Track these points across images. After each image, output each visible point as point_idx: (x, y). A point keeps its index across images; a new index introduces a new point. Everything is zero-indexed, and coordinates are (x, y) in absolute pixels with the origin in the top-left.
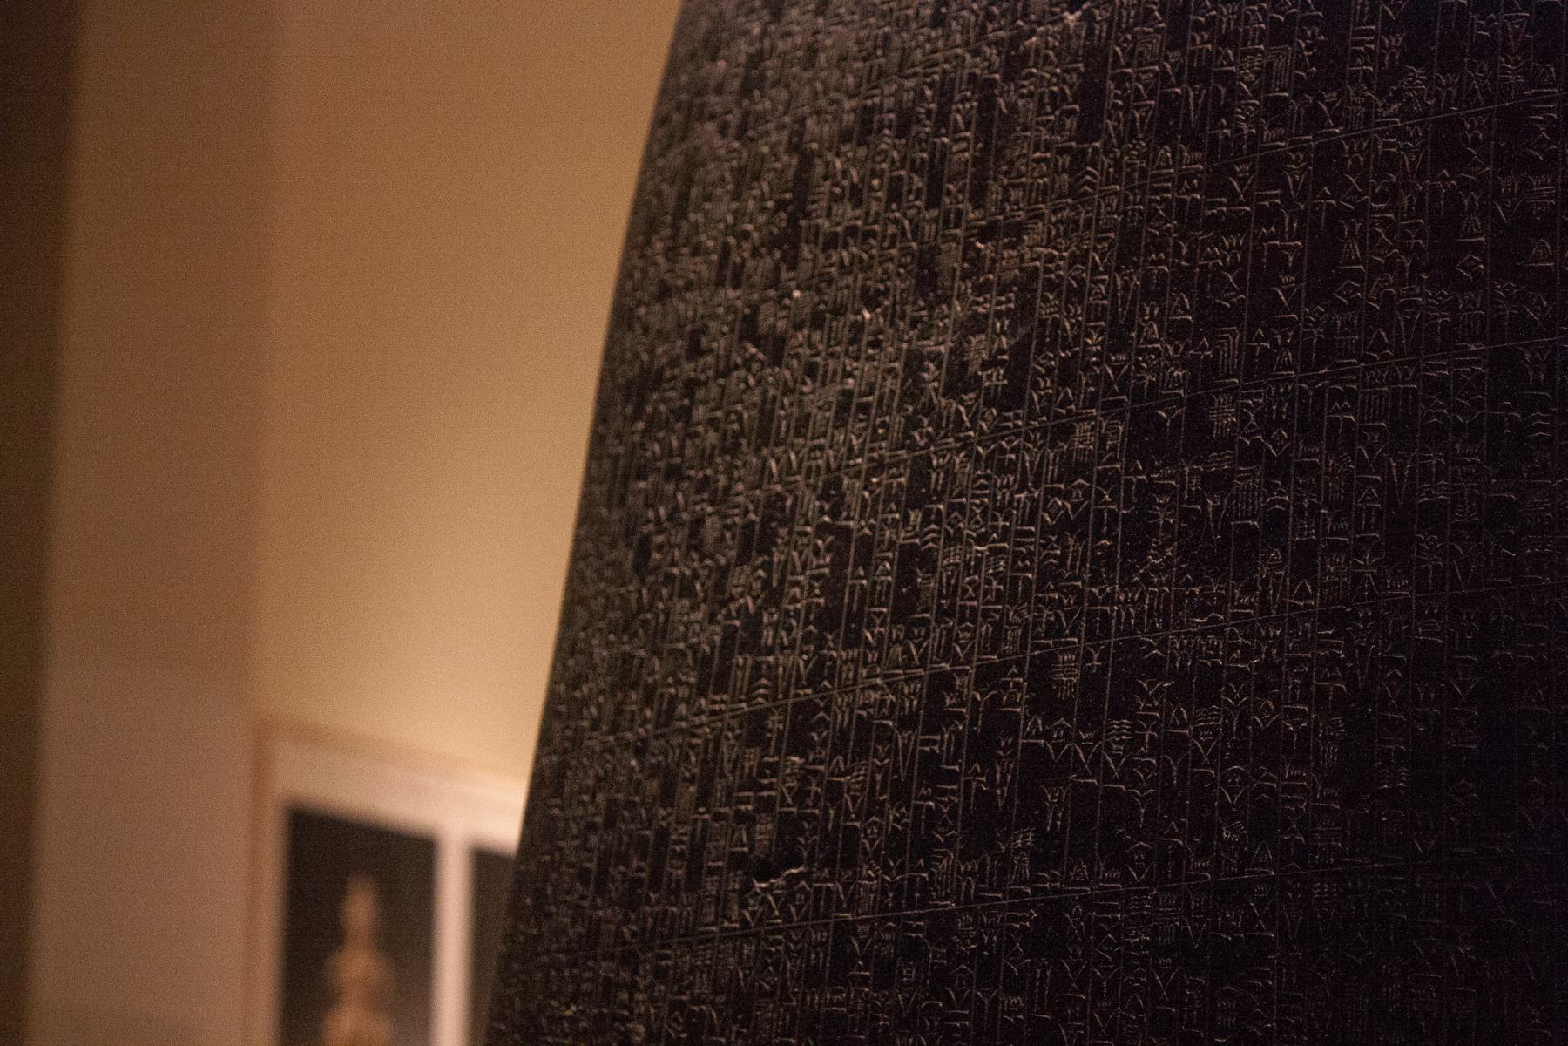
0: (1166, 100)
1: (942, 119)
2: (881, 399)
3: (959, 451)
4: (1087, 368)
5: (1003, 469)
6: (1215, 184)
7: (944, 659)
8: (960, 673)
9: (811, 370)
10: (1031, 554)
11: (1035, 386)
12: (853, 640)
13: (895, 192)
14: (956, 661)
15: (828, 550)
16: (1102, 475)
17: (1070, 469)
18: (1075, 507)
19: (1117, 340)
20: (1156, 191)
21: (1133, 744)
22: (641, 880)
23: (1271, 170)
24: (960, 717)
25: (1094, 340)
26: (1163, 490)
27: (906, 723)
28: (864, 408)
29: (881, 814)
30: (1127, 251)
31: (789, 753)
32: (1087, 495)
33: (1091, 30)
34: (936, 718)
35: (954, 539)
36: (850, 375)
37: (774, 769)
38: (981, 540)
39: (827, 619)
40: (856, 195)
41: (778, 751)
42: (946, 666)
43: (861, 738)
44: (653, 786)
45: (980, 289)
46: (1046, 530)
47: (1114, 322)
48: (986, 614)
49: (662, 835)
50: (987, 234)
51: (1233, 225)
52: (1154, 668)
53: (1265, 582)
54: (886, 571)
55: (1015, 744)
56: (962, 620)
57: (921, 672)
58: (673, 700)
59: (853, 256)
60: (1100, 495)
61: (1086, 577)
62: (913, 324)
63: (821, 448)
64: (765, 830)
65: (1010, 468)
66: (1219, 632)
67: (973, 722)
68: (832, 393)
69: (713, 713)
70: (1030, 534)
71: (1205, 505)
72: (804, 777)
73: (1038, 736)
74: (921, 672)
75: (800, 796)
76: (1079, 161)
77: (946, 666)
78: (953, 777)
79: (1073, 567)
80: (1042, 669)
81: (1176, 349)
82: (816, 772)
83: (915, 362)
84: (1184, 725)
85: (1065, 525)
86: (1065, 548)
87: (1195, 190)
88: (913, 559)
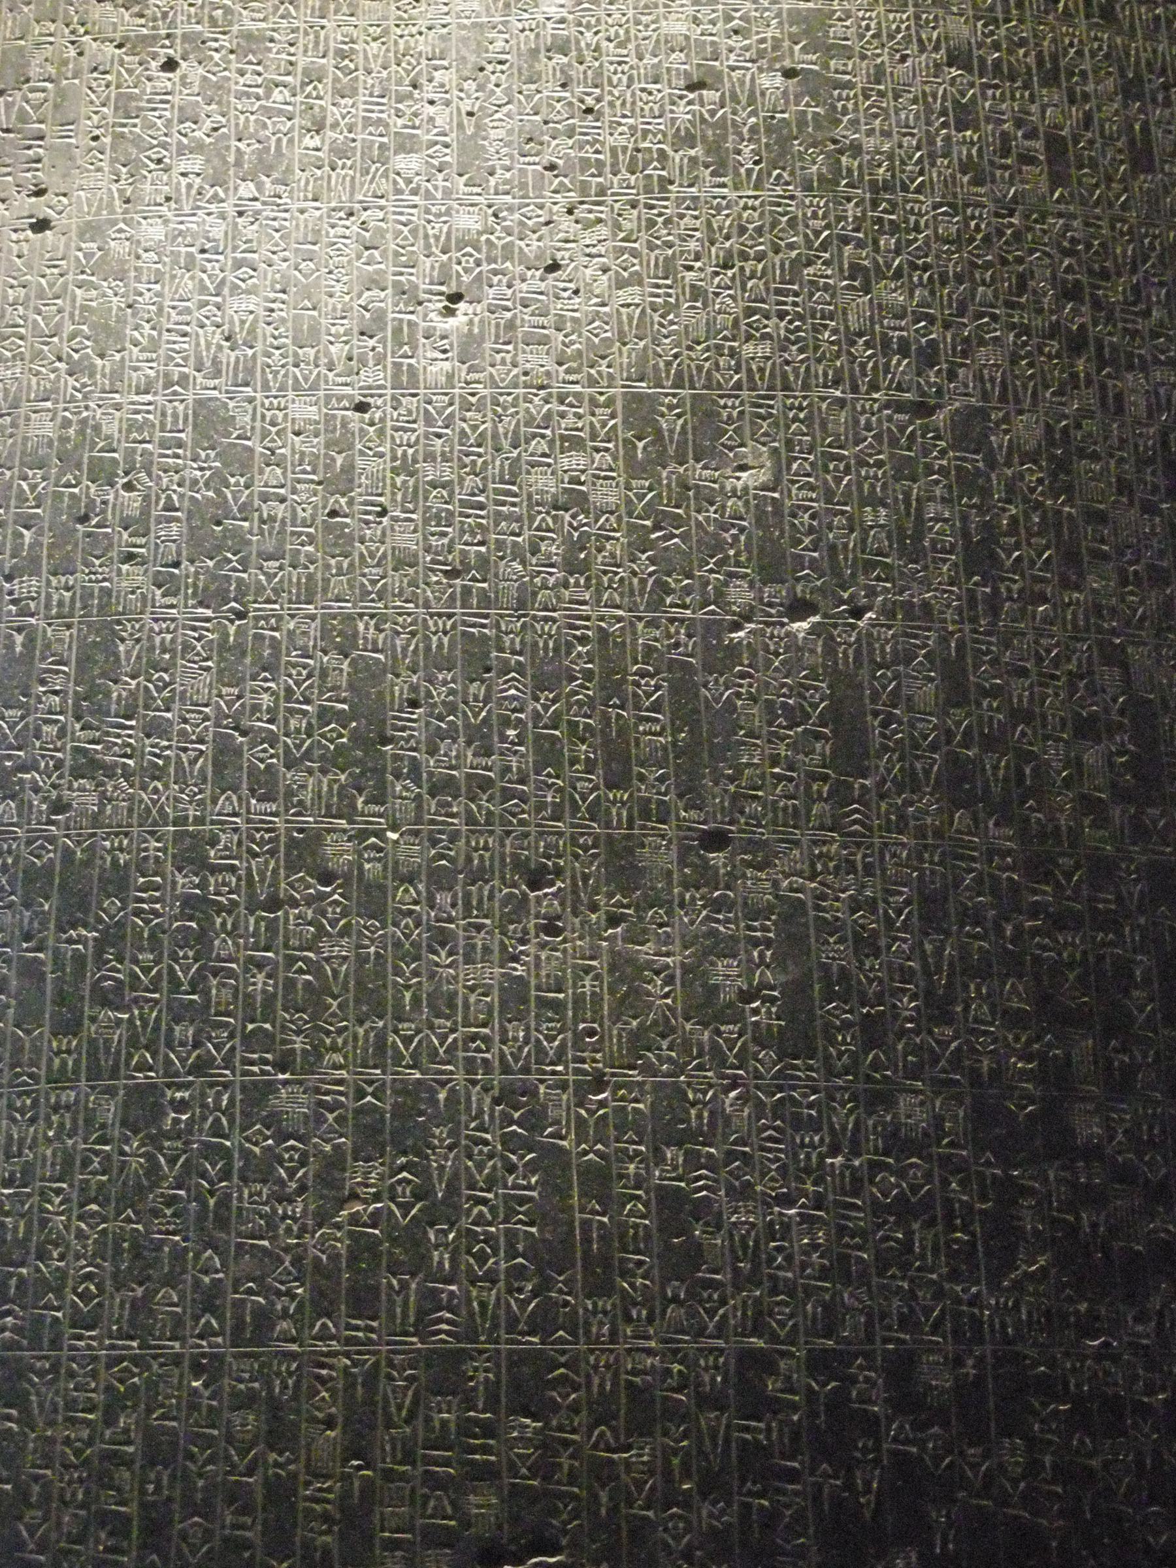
0: (953, 760)
1: (612, 685)
2: (579, 1000)
3: (727, 1090)
4: (903, 1032)
5: (798, 1123)
6: (1039, 868)
7: (756, 1331)
8: (783, 1354)
9: (442, 938)
10: (863, 1233)
11: (832, 1041)
12: (600, 1287)
13: (548, 754)
14: (774, 1338)
15: (532, 1168)
16: (945, 1161)
17: (898, 1143)
18: (914, 1189)
19: (938, 1008)
20: (962, 858)
21: (1033, 1467)
22: (247, 1545)
23: (1102, 870)
24: (794, 1407)
25: (908, 1005)
26: (1031, 1192)
27: (704, 1401)
28: (557, 1006)
29: (686, 1505)
30: (932, 909)
31: (513, 1411)
32: (928, 1176)
33: (830, 649)
34: (758, 1405)
35: (744, 1192)
36: (515, 959)
37: (488, 1430)
38: (787, 1201)
39: (549, 1259)
40: (481, 739)
41: (492, 1403)
42: (761, 1344)
43: (642, 1410)
44: (249, 1422)
45: (717, 905)
46: (877, 1208)
47: (929, 993)
48: (808, 1292)
49: (280, 1493)
50: (716, 840)
51: (1059, 922)
52: (1050, 1389)
53: (1161, 1314)
54: (638, 1215)
55: (877, 1449)
56: (774, 1291)
57: (720, 1343)
58: (264, 1319)
59: (490, 813)
60: (945, 1183)
61: (945, 1270)
62: (614, 920)
63: (486, 1039)
64: (483, 1504)
65: (815, 1126)
66: (1115, 1359)
67: (813, 1414)
68: (493, 973)
69: (349, 1341)
70: (854, 1207)
71: (1078, 1218)
72: (547, 1445)
73: (907, 1442)
74: (720, 1343)
75: (545, 1469)
76: (841, 795)
77: (757, 1342)
78: (793, 1476)
79: (923, 1257)
80: (901, 1369)
81: (1017, 1039)
82: (566, 1443)
83: (625, 969)
84: (1090, 1455)
85: (903, 1210)
86: (909, 1234)
87: (1008, 868)
88: (673, 1207)
